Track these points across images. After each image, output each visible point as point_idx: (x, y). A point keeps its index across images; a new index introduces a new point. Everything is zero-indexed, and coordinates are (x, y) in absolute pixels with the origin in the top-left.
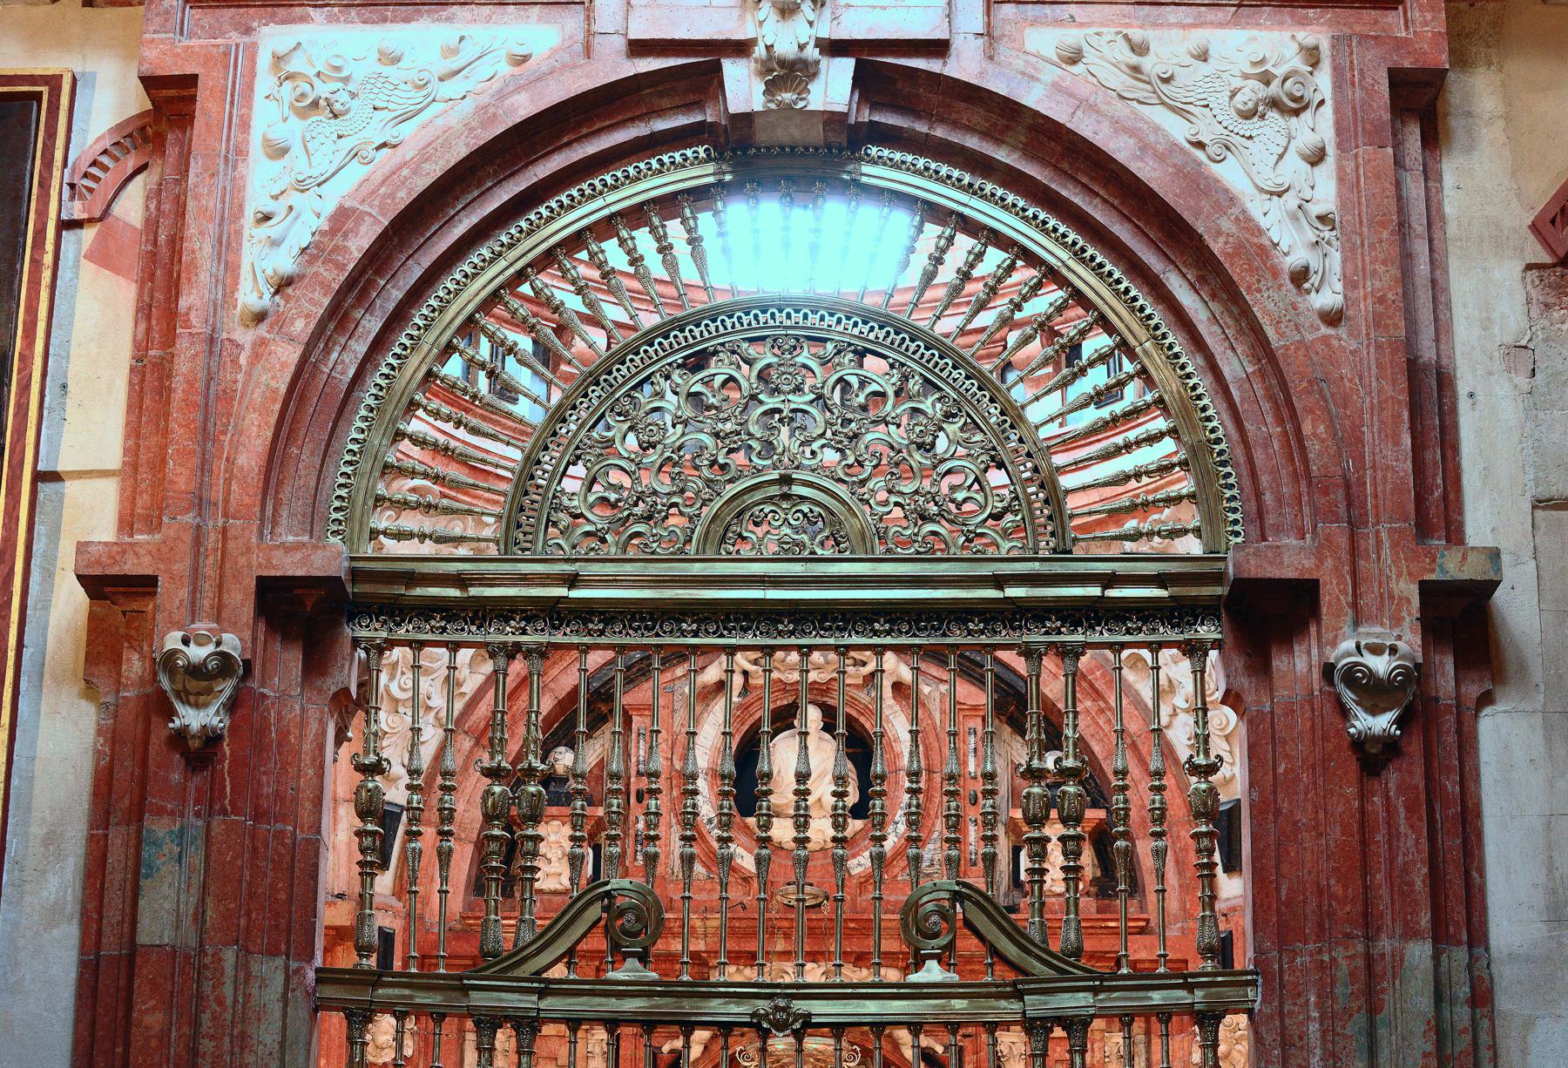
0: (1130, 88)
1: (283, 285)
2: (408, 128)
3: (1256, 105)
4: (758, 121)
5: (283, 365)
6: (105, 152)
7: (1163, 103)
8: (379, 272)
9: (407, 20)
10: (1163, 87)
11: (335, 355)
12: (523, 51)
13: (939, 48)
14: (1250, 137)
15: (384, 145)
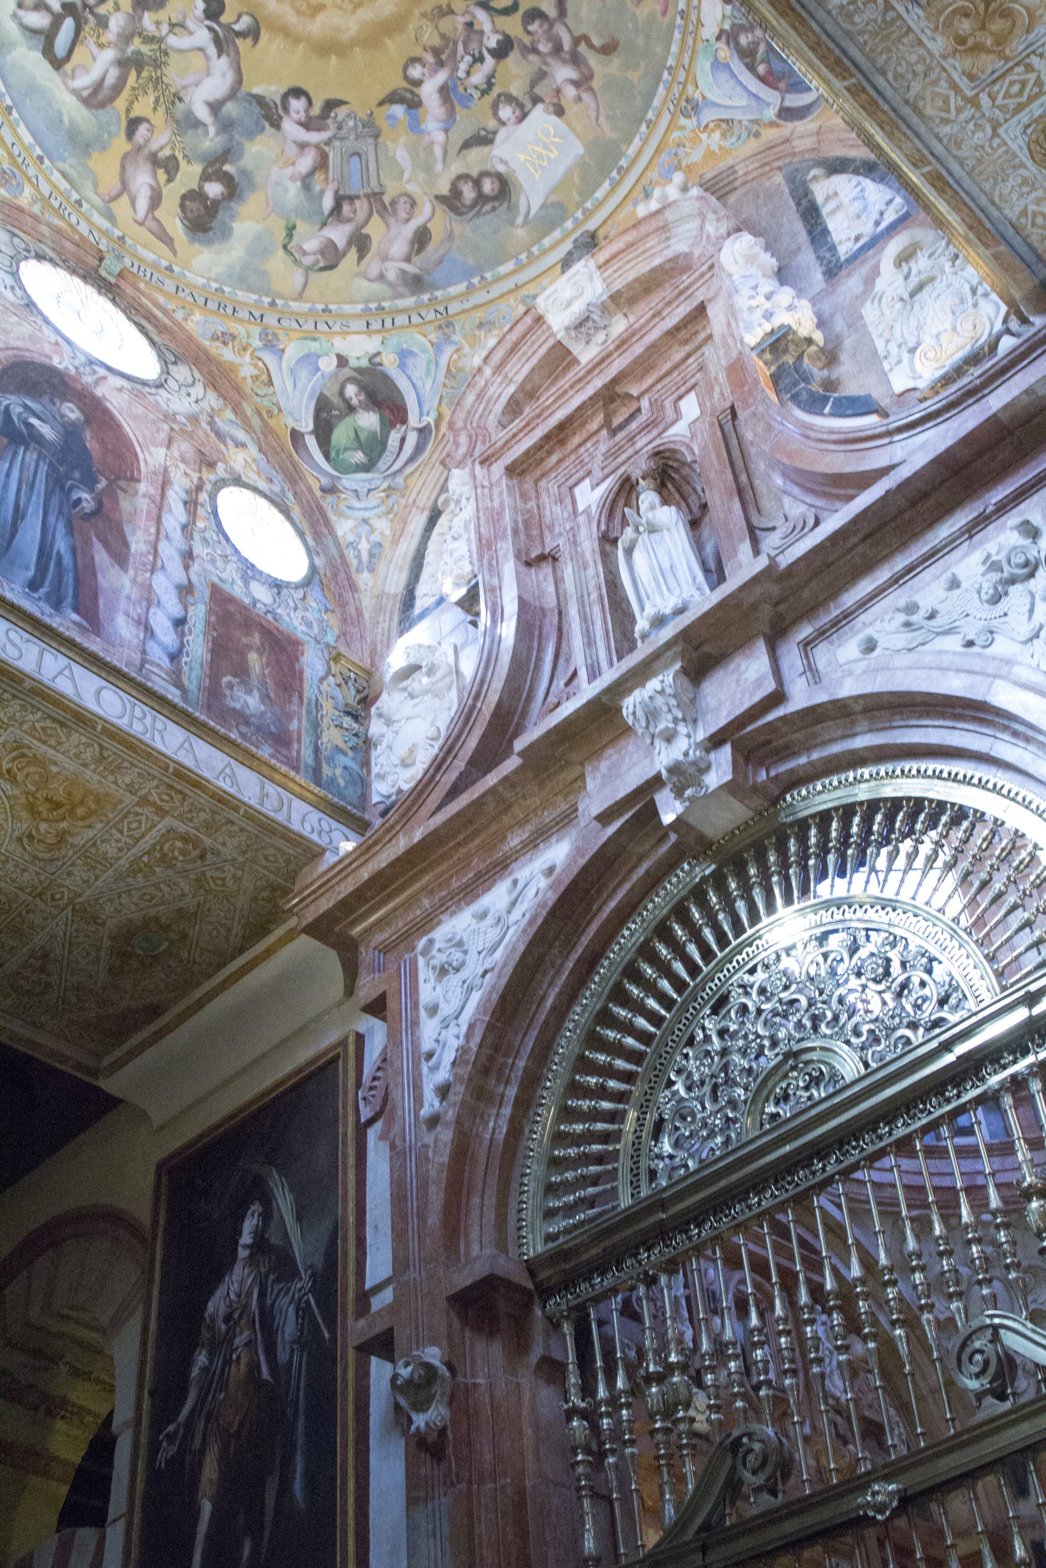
0: (912, 640)
1: (443, 1091)
2: (499, 954)
3: (996, 589)
4: (691, 820)
5: (445, 1144)
6: (379, 1069)
7: (938, 634)
8: (507, 1055)
9: (489, 889)
10: (933, 623)
11: (491, 1124)
12: (547, 865)
13: (777, 698)
14: (1006, 614)
15: (485, 972)
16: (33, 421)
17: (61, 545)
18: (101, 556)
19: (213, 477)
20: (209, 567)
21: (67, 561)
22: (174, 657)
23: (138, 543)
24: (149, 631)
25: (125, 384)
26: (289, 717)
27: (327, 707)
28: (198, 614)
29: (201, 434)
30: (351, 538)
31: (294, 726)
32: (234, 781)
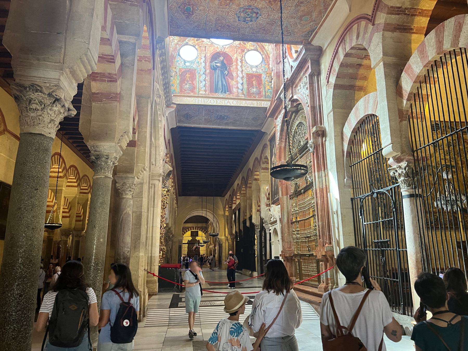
16: (217, 64)
17: (224, 83)
18: (230, 80)
19: (244, 53)
20: (246, 71)
21: (225, 85)
22: (242, 90)
23: (234, 74)
24: (238, 88)
25: (228, 46)
26: (260, 89)
27: (266, 83)
28: (245, 80)
29: (241, 46)
30: (268, 49)
31: (261, 89)
32: (253, 104)
